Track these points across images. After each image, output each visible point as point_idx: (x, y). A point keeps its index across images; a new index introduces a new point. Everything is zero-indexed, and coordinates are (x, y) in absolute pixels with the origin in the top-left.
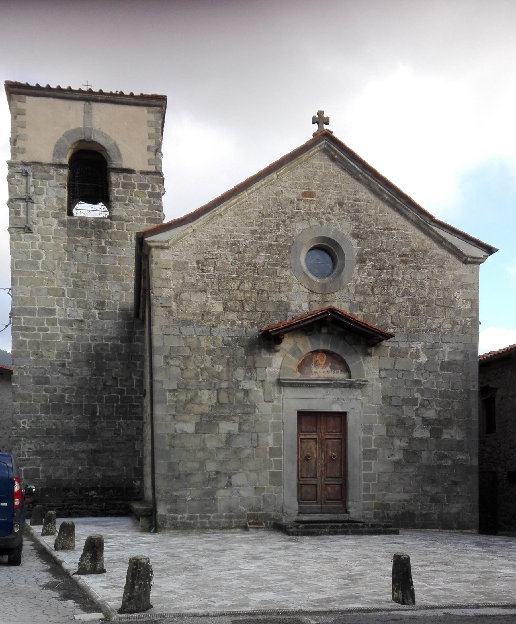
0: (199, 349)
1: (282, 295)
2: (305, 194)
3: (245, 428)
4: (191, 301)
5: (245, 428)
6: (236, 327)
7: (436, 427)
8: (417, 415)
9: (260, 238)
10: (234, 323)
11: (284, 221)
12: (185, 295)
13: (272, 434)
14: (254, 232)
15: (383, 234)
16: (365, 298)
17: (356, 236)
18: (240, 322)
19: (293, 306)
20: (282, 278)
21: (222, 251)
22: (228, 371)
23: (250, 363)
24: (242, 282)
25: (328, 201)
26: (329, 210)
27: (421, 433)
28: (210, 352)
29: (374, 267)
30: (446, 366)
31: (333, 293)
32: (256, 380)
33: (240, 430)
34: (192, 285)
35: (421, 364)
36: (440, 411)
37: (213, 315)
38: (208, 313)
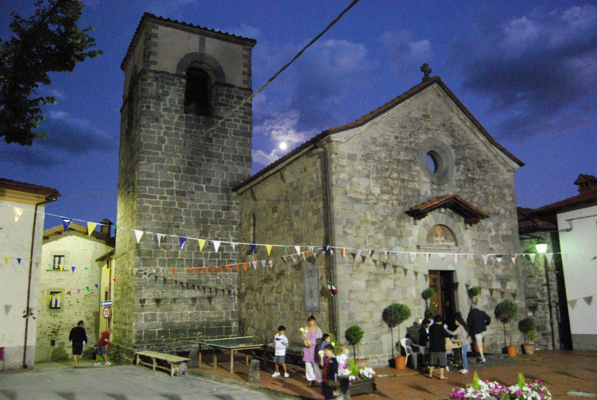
0: (366, 221)
1: (416, 183)
2: (424, 116)
3: (398, 283)
4: (359, 184)
5: (398, 283)
6: (389, 205)
7: (503, 281)
8: (493, 272)
9: (400, 142)
10: (388, 202)
11: (414, 132)
12: (355, 179)
13: (415, 288)
14: (396, 138)
15: (467, 148)
16: (461, 190)
17: (453, 147)
18: (391, 202)
19: (422, 193)
20: (415, 171)
21: (378, 149)
22: (386, 239)
23: (399, 233)
24: (391, 172)
25: (437, 122)
26: (438, 128)
27: (496, 285)
28: (374, 223)
29: (464, 169)
30: (505, 237)
31: (444, 184)
32: (403, 246)
33: (395, 285)
34: (359, 172)
35: (492, 236)
36: (504, 269)
37: (374, 195)
38: (371, 194)
